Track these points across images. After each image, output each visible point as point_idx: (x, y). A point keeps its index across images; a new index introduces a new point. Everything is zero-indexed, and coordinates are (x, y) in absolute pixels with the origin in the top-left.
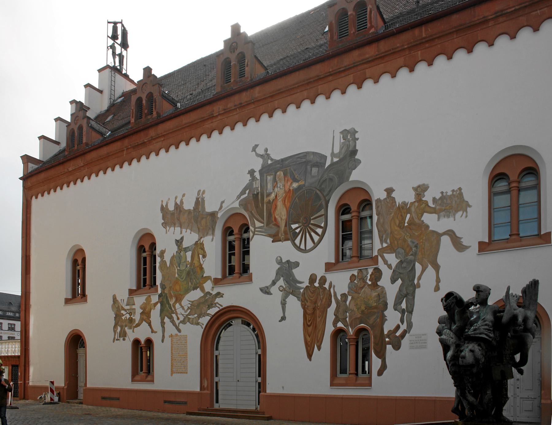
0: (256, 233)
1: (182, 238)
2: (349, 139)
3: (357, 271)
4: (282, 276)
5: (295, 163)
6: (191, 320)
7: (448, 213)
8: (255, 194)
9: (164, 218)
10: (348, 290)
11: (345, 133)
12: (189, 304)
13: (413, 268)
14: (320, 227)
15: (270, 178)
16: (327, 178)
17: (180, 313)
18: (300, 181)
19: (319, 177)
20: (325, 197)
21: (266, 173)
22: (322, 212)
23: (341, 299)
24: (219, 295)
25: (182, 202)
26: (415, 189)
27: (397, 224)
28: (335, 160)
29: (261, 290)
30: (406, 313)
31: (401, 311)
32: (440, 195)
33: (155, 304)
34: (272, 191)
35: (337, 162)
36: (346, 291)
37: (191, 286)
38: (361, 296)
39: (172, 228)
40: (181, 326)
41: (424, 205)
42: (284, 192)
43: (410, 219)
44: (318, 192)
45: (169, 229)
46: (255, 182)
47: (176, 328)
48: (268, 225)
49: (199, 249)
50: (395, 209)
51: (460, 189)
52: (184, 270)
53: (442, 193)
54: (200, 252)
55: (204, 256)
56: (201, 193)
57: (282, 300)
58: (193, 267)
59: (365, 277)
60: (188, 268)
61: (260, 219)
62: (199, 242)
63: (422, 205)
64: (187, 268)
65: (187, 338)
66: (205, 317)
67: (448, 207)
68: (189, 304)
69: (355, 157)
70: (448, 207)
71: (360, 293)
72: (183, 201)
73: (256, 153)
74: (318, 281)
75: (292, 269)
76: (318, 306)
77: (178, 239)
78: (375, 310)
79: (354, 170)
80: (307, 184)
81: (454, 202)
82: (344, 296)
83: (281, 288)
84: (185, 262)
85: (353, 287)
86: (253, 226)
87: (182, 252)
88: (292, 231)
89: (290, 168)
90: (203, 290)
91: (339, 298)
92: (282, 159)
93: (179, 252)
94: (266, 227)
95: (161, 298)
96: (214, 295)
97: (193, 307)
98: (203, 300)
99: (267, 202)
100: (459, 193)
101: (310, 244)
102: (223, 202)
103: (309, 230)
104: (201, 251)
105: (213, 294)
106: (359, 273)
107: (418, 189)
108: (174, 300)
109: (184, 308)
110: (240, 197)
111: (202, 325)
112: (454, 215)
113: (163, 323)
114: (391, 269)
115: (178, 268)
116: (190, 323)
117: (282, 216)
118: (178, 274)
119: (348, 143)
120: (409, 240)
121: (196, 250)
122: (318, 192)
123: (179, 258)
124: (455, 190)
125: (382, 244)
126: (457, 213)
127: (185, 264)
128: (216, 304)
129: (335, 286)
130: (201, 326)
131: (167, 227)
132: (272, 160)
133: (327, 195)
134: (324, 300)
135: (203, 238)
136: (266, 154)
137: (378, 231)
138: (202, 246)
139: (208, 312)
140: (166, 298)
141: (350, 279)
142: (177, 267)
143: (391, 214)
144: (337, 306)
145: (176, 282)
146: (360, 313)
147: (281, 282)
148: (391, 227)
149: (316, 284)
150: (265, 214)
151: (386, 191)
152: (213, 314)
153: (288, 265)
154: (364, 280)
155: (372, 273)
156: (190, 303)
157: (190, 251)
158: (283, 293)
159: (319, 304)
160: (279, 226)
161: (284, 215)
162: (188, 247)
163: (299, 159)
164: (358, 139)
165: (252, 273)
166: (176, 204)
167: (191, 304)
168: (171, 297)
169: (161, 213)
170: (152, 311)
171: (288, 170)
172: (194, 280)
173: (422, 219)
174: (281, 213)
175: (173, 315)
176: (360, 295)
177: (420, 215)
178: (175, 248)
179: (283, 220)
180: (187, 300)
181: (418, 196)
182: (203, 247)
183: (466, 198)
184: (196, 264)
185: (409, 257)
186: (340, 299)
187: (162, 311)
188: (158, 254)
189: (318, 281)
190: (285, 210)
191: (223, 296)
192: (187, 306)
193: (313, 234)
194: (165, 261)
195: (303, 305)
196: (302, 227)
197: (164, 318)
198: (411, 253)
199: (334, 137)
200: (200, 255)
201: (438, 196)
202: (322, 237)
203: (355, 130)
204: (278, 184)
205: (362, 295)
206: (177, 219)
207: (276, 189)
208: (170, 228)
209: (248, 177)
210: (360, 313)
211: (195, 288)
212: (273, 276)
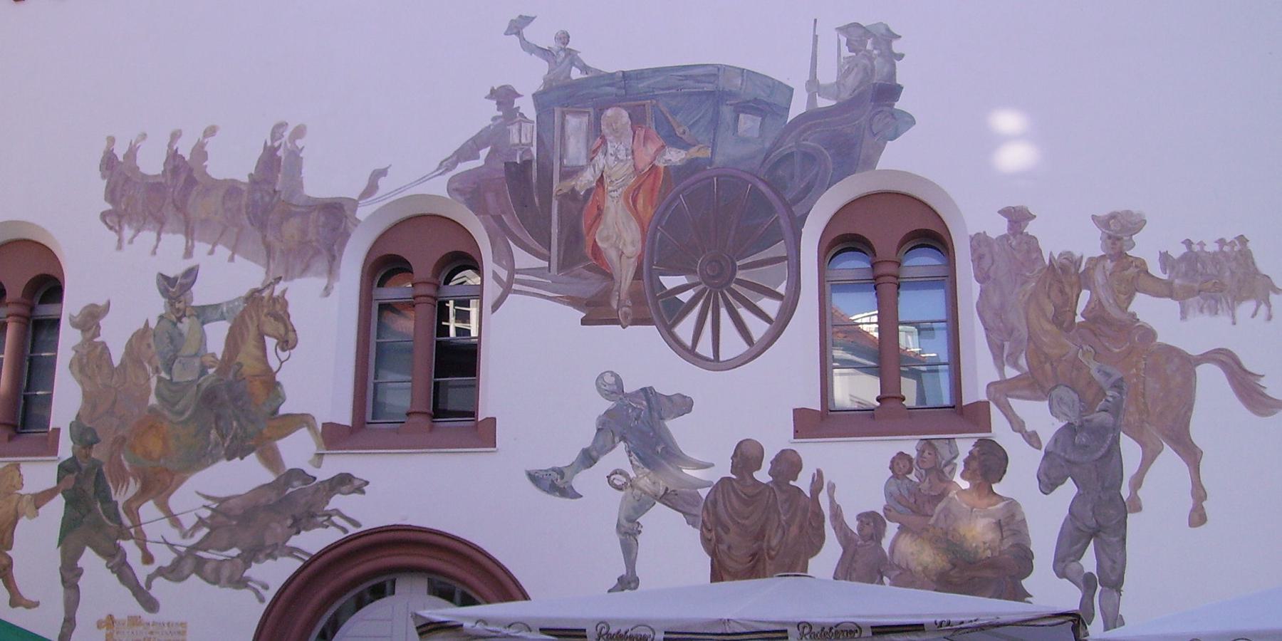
0: (515, 287)
1: (191, 274)
2: (869, 52)
3: (917, 442)
4: (623, 438)
5: (674, 91)
6: (209, 568)
7: (1213, 302)
8: (516, 163)
9: (111, 195)
10: (885, 503)
11: (855, 34)
12: (204, 506)
13: (1113, 452)
14: (774, 295)
15: (576, 124)
16: (794, 149)
17: (162, 541)
18: (695, 146)
19: (767, 145)
20: (788, 206)
21: (563, 106)
22: (779, 249)
23: (860, 529)
24: (344, 482)
25: (200, 152)
26: (1104, 222)
27: (1050, 315)
28: (823, 103)
29: (534, 478)
30: (1099, 588)
31: (1080, 580)
32: (1184, 249)
33: (41, 499)
34: (583, 162)
35: (827, 112)
36: (877, 503)
37: (217, 445)
38: (934, 527)
39: (148, 236)
40: (161, 588)
41: (1132, 271)
42: (631, 170)
43: (1093, 305)
44: (762, 187)
45: (135, 236)
46: (517, 126)
47: (134, 594)
48: (562, 267)
49: (263, 318)
50: (1040, 271)
51: (1242, 240)
52: (192, 382)
53: (1188, 243)
54: (267, 328)
55: (287, 342)
56: (287, 134)
57: (624, 522)
58: (235, 376)
59: (945, 466)
60: (210, 380)
61: (534, 244)
62: (266, 294)
63: (1127, 270)
64: (202, 379)
65: (184, 633)
66: (275, 559)
67: (1210, 285)
68: (204, 506)
69: (891, 106)
70: (1210, 285)
71: (932, 516)
72: (206, 148)
73: (522, 40)
74: (766, 465)
75: (662, 419)
76: (769, 548)
77: (171, 275)
78: (989, 573)
79: (891, 140)
80: (719, 160)
81: (1228, 274)
82: (872, 522)
83: (618, 476)
84: (196, 355)
85: (905, 493)
86: (504, 263)
87: (184, 320)
88: (661, 297)
89: (654, 102)
90: (272, 460)
91: (853, 525)
92: (623, 72)
93: (173, 318)
94: (558, 273)
95: (71, 478)
96: (322, 482)
97: (221, 519)
98: (273, 497)
99: (565, 195)
100: (1240, 251)
101: (732, 344)
102: (383, 173)
103: (730, 297)
104: (270, 325)
105: (319, 479)
106: (924, 452)
107: (1111, 222)
108: (133, 487)
109: (178, 520)
110: (455, 164)
111: (259, 588)
112: (1232, 309)
113: (70, 575)
114: (1039, 448)
115: (163, 374)
116: (205, 579)
117: (624, 244)
118: (158, 394)
119: (866, 61)
120: (1093, 367)
121: (251, 318)
122: (762, 187)
123: (172, 340)
124: (1228, 240)
125: (1001, 370)
126: (1239, 304)
127: (197, 362)
128: (330, 516)
129: (834, 486)
130: (257, 592)
131: (126, 227)
132: (585, 68)
133: (796, 201)
134: (794, 530)
135: (285, 280)
136: (565, 50)
137: (986, 329)
138: (278, 307)
139: (294, 541)
140: (94, 477)
141: (891, 468)
142: (157, 370)
143: (1025, 282)
144: (844, 552)
145: (152, 422)
146: (932, 580)
147: (618, 458)
148: (1027, 319)
149: (763, 476)
150: (555, 230)
151: (1005, 216)
152: (315, 550)
153: (645, 403)
154: (945, 476)
155: (970, 453)
156: (209, 503)
157: (223, 318)
158: (625, 498)
159: (774, 542)
160: (610, 276)
161: (633, 243)
162: (217, 306)
163: (690, 83)
164: (901, 57)
165: (493, 420)
166: (173, 156)
167: (213, 510)
168: (121, 478)
169: (104, 177)
170: (23, 522)
171: (649, 110)
172: (235, 424)
173: (1131, 309)
174: (619, 236)
175: (123, 543)
176: (932, 521)
177: (1123, 297)
178: (156, 306)
179: (628, 258)
180: (198, 493)
181: (1114, 244)
182: (281, 313)
183: (1263, 265)
184: (244, 367)
185: (1095, 415)
186: (856, 531)
187: (68, 527)
188: (71, 318)
189: (766, 465)
190: (634, 225)
191: (365, 488)
192: (196, 514)
193: (744, 313)
194: (103, 343)
195: (710, 540)
196: (701, 287)
197: (80, 553)
198: (1102, 404)
199: (816, 38)
200: (266, 338)
201: (1177, 251)
202: (779, 326)
203: (888, 30)
204: (609, 145)
205: (937, 519)
206: (175, 205)
207: (600, 160)
208: (138, 231)
209: (491, 110)
210: (935, 578)
211: (237, 451)
212: (586, 436)
